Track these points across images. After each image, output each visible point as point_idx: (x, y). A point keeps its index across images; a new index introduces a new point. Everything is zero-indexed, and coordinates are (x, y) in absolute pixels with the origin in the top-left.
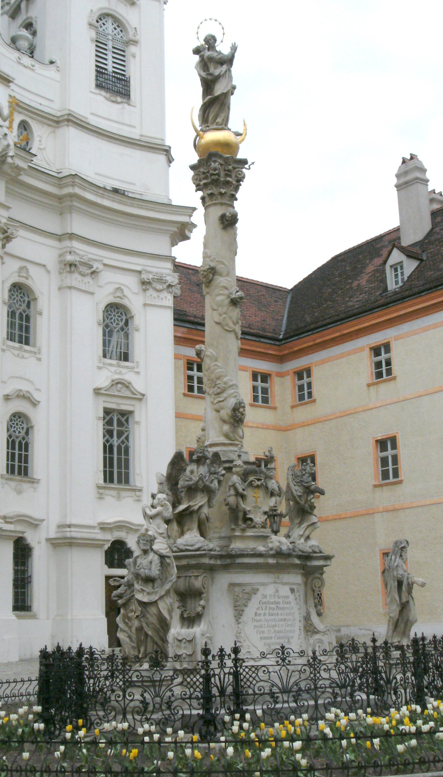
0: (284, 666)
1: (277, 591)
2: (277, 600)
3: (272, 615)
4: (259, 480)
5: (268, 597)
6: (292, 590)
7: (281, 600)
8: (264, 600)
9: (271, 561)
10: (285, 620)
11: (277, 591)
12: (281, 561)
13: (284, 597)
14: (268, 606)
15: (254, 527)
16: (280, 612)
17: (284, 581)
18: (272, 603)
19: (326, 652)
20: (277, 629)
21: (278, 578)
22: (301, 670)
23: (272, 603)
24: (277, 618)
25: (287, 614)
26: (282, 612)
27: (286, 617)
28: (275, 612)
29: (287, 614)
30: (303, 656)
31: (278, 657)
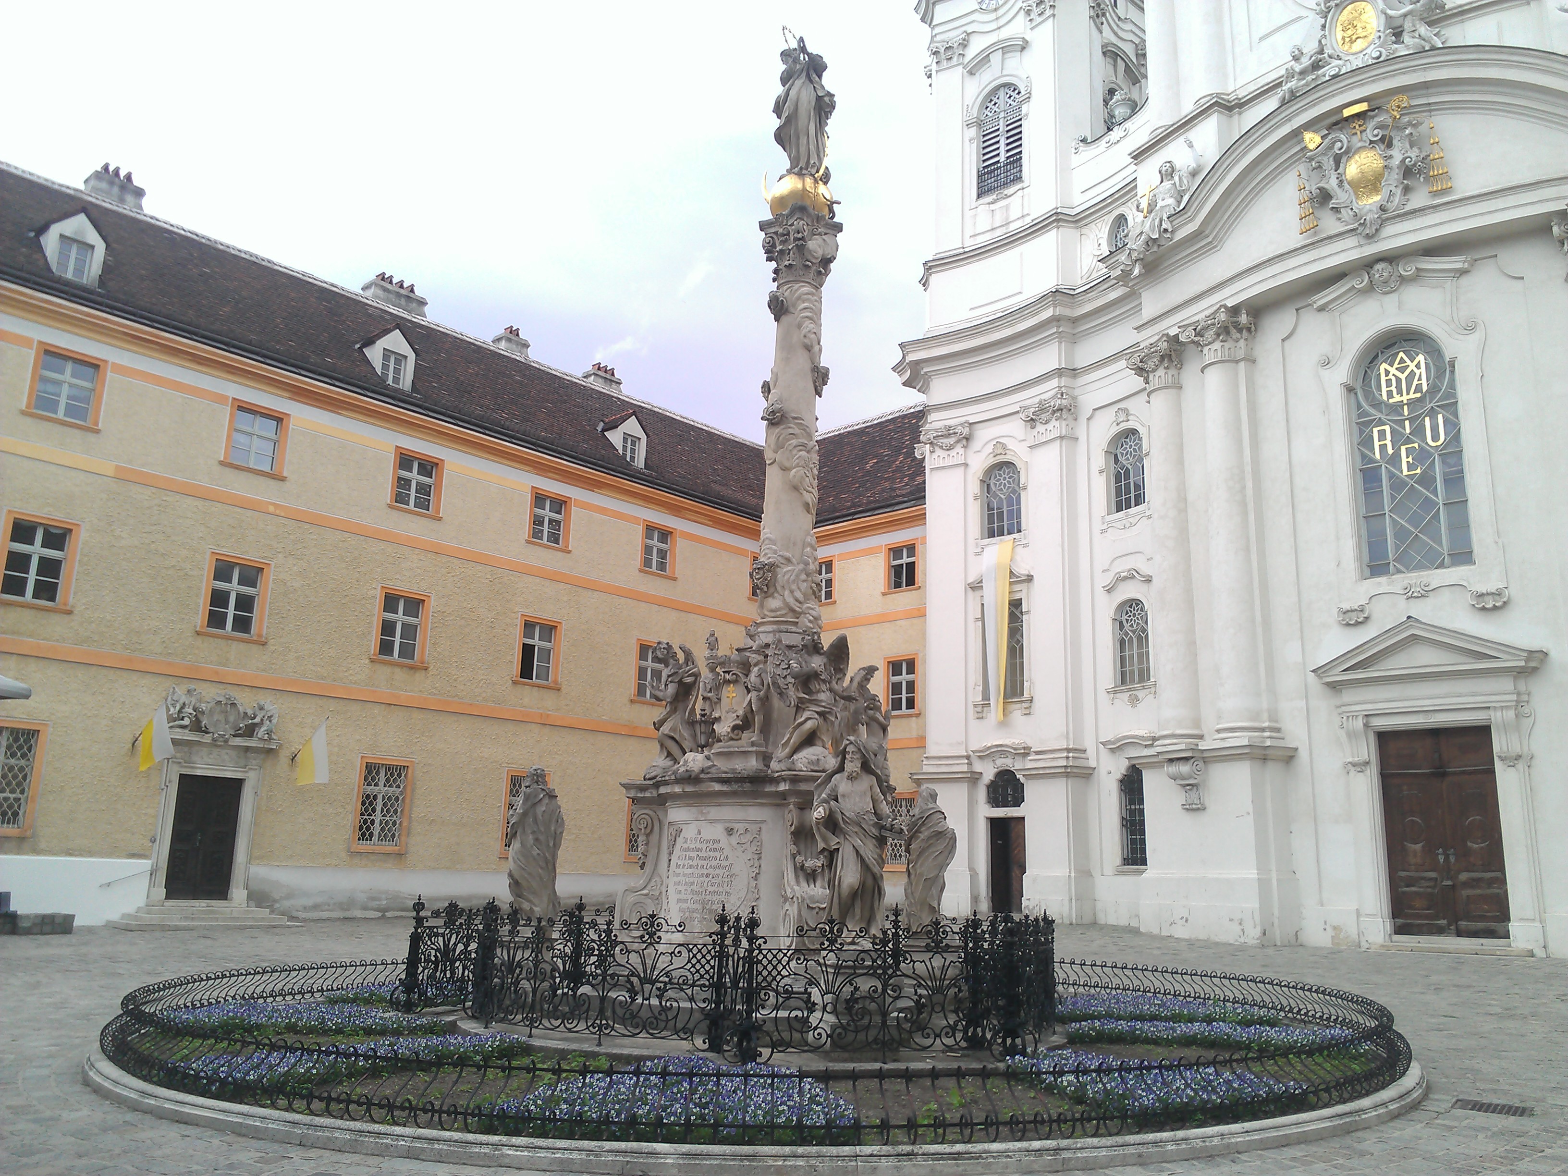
0: (832, 951)
1: (699, 833)
2: (698, 845)
3: (691, 867)
4: (728, 672)
5: (689, 841)
6: (730, 831)
7: (704, 846)
8: (685, 846)
9: (677, 789)
10: (707, 876)
11: (699, 833)
12: (689, 789)
13: (708, 841)
14: (687, 854)
15: (719, 741)
16: (701, 863)
17: (711, 816)
18: (693, 850)
19: (626, 924)
20: (694, 887)
21: (702, 813)
22: (673, 952)
23: (693, 850)
24: (696, 871)
25: (715, 868)
26: (705, 863)
27: (711, 871)
28: (694, 863)
29: (715, 868)
30: (626, 929)
31: (929, 938)
